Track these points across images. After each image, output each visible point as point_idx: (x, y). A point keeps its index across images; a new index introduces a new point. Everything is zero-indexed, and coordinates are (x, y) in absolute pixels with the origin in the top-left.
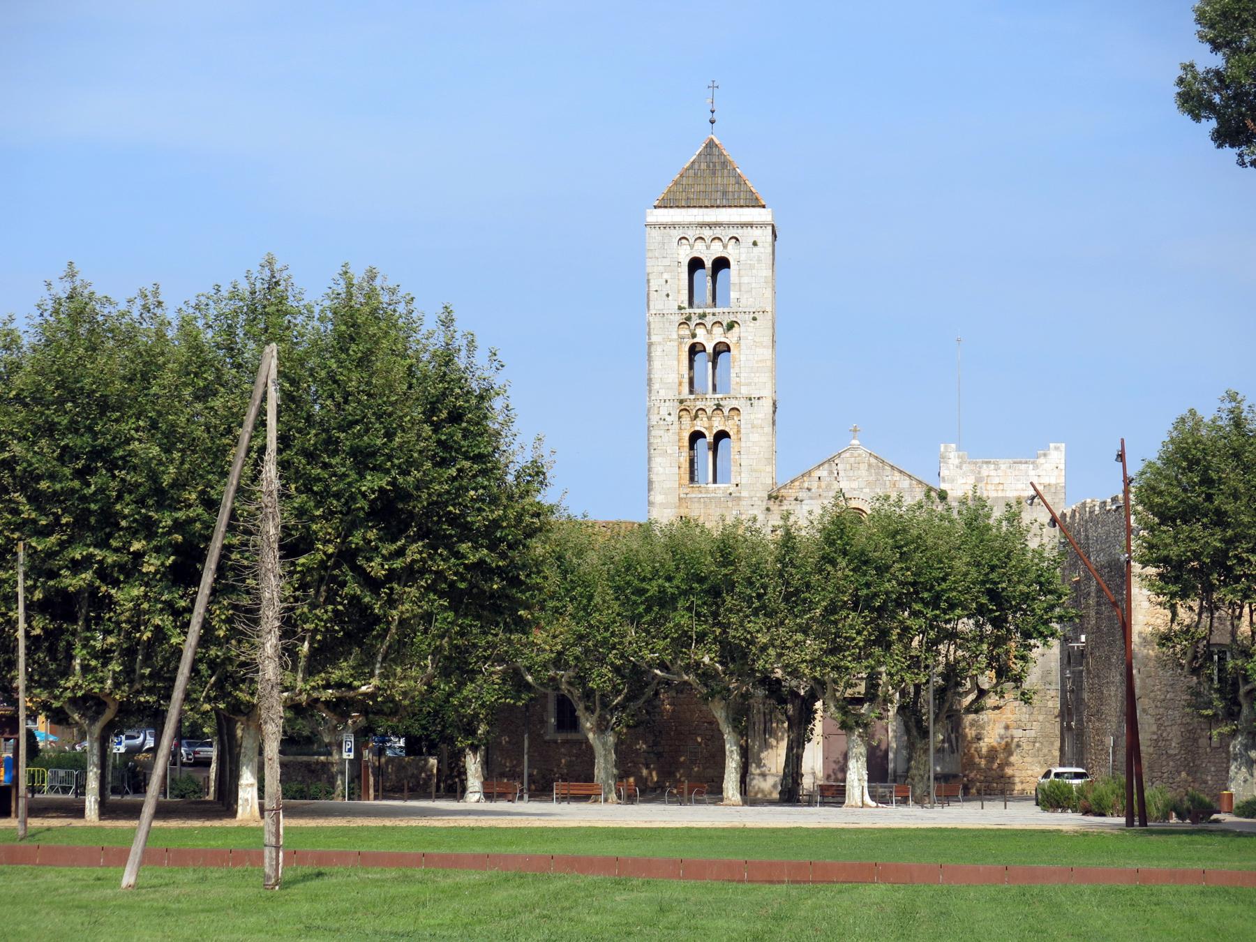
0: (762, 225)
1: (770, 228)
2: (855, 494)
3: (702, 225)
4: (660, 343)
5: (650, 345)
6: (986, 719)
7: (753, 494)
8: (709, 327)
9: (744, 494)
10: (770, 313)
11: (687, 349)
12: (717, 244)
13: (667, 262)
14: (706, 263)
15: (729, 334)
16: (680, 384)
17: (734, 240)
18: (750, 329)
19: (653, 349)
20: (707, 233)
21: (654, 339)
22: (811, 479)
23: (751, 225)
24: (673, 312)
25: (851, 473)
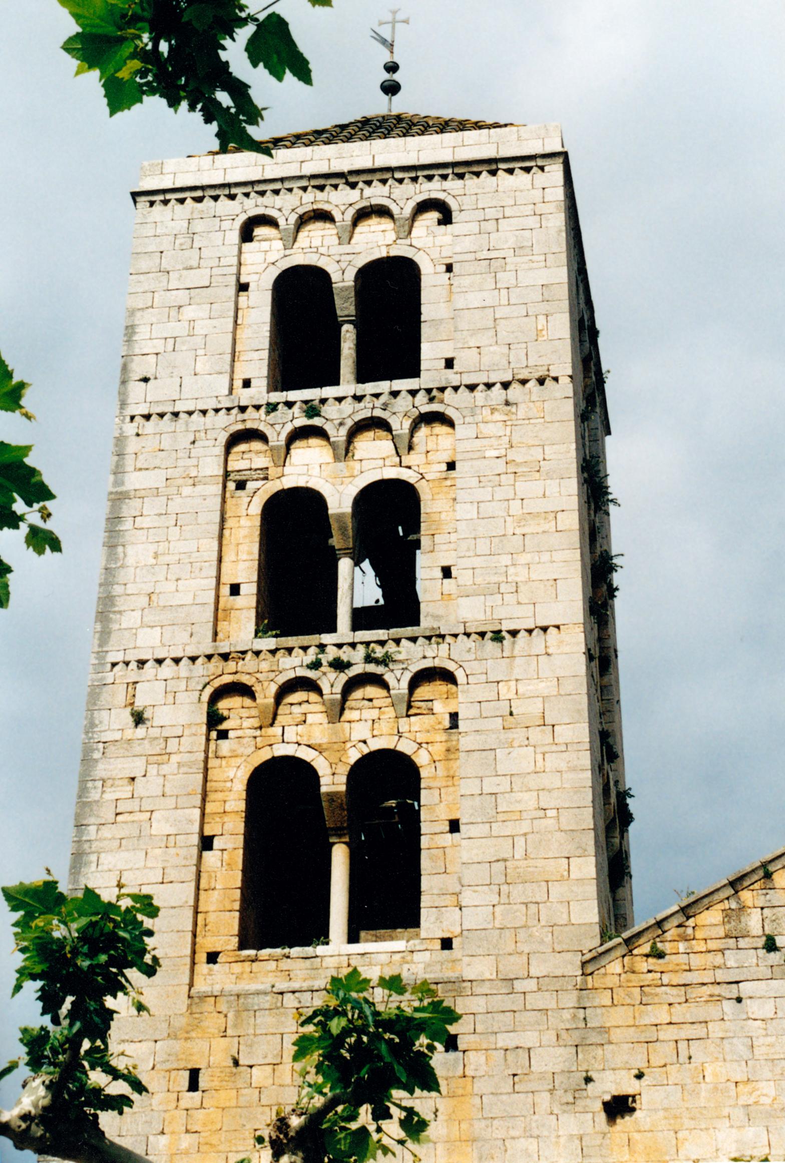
5: (119, 498)
7: (513, 966)
8: (339, 435)
10: (565, 381)
11: (256, 508)
12: (374, 228)
13: (199, 278)
14: (335, 277)
15: (409, 459)
17: (433, 216)
18: (487, 429)
19: (129, 509)
21: (133, 481)
23: (492, 165)
24: (210, 404)
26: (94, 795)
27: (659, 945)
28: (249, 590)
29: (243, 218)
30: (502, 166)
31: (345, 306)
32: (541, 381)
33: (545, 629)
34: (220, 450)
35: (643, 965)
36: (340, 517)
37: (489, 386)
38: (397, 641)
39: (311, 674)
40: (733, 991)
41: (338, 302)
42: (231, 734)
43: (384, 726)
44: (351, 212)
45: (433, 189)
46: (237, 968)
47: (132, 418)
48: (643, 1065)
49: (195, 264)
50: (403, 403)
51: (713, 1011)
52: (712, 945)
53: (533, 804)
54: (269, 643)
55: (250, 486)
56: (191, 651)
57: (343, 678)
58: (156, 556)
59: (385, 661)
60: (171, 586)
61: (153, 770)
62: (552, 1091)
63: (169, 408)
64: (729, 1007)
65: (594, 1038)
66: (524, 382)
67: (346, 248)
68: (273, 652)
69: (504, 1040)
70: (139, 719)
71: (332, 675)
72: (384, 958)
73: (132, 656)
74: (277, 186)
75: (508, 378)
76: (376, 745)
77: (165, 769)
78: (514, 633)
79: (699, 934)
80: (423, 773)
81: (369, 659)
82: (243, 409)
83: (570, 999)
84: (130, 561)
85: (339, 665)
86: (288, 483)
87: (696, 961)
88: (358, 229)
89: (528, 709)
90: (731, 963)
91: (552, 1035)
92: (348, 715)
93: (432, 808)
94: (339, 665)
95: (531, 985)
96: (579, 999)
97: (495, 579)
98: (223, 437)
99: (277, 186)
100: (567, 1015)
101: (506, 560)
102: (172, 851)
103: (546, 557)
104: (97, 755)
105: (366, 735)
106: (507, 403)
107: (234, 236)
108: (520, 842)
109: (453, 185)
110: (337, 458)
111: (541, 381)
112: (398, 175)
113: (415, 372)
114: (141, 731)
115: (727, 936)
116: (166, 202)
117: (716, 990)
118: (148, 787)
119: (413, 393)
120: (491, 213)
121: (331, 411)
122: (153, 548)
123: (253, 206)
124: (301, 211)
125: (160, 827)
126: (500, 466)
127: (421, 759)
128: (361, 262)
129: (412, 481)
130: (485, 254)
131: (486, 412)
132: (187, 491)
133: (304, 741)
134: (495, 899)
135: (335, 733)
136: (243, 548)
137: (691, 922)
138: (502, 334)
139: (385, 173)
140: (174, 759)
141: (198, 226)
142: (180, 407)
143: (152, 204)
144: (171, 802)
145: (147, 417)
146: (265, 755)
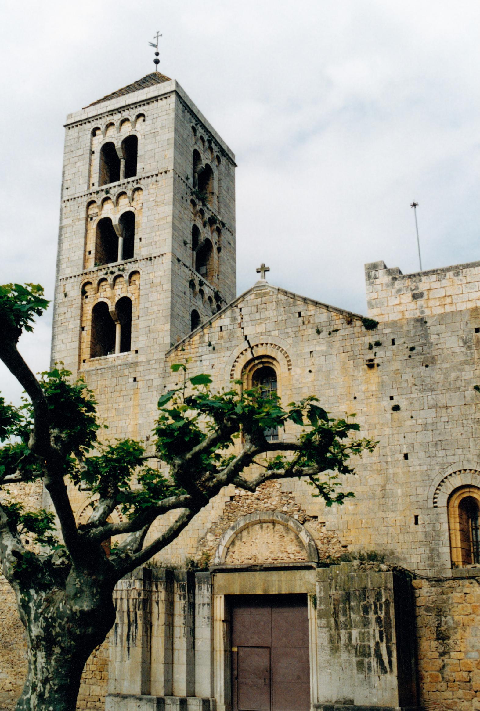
0: (165, 96)
1: (173, 97)
2: (263, 339)
3: (112, 112)
4: (70, 225)
6: (451, 623)
7: (150, 357)
9: (141, 358)
10: (172, 171)
12: (127, 125)
13: (80, 152)
14: (116, 145)
15: (134, 203)
16: (85, 260)
18: (152, 191)
20: (117, 118)
22: (212, 330)
23: (156, 99)
24: (82, 194)
25: (257, 316)
26: (56, 319)
27: (184, 347)
28: (93, 252)
29: (92, 129)
30: (159, 98)
31: (120, 154)
32: (166, 172)
33: (162, 255)
34: (84, 209)
35: (180, 353)
36: (116, 225)
37: (152, 176)
38: (126, 263)
39: (105, 277)
40: (200, 359)
41: (118, 153)
42: (89, 297)
43: (124, 290)
44: (119, 122)
45: (140, 110)
46: (90, 363)
47: (64, 201)
48: (177, 381)
49: (79, 147)
50: (130, 186)
51: (195, 365)
52: (197, 346)
53: (156, 309)
54: (96, 268)
55: (94, 218)
56: (78, 273)
57: (113, 276)
58: (70, 245)
59: (123, 270)
60: (73, 254)
61: (69, 310)
62: (157, 391)
63: (73, 197)
64: (199, 363)
65: (167, 375)
66: (161, 173)
67: (119, 134)
68: (97, 271)
69: (147, 378)
70: (66, 295)
71: (110, 276)
72: (122, 357)
73: (64, 277)
74: (100, 116)
75: (157, 173)
76: (122, 295)
77: (72, 309)
78: (155, 257)
79: (193, 343)
80: (133, 303)
81: (119, 270)
82: (91, 194)
83: (162, 365)
84: (64, 248)
85: (112, 273)
86: (103, 216)
87: (192, 351)
88: (123, 127)
89: (157, 281)
90: (200, 351)
91: (157, 375)
92: (116, 287)
93: (135, 313)
94: (112, 273)
95: (153, 362)
96: (165, 364)
97: (151, 241)
98: (86, 204)
99: (100, 116)
100: (161, 369)
101: (154, 234)
102: (74, 333)
103: (163, 232)
104: (57, 307)
105: (120, 293)
106: (156, 181)
107: (89, 136)
108: (153, 321)
109: (146, 107)
110: (115, 207)
111: (166, 172)
112: (132, 107)
113: (135, 175)
114: (66, 299)
115: (200, 343)
116: (73, 127)
117: (196, 359)
118: (68, 315)
119: (133, 181)
120: (155, 116)
121: (112, 191)
122: (69, 243)
123: (94, 125)
124: (106, 124)
125: (71, 326)
126: (154, 203)
127: (133, 299)
128: (123, 138)
129: (133, 211)
130: (154, 131)
131: (151, 185)
132: (77, 223)
133: (105, 296)
134: (146, 338)
135: (113, 293)
136: (92, 239)
137: (192, 340)
138: (156, 158)
139: (127, 107)
140: (74, 306)
141: (81, 134)
142: (76, 196)
143: (69, 128)
144: (73, 319)
145: (68, 200)
146: (96, 302)
